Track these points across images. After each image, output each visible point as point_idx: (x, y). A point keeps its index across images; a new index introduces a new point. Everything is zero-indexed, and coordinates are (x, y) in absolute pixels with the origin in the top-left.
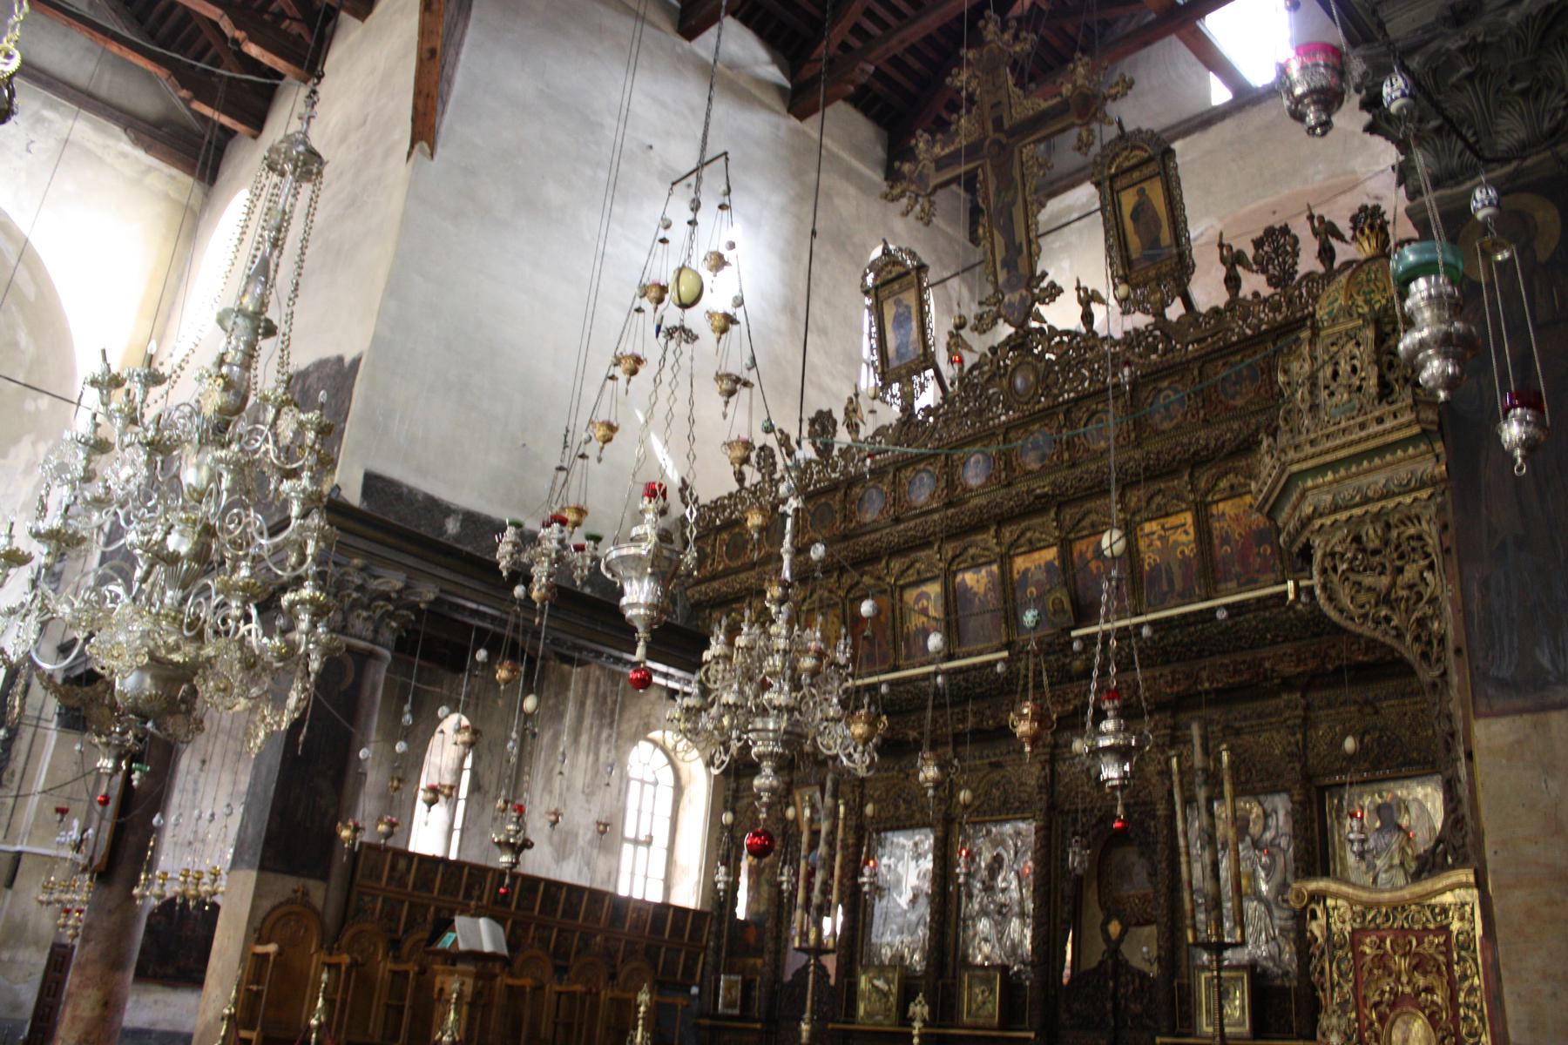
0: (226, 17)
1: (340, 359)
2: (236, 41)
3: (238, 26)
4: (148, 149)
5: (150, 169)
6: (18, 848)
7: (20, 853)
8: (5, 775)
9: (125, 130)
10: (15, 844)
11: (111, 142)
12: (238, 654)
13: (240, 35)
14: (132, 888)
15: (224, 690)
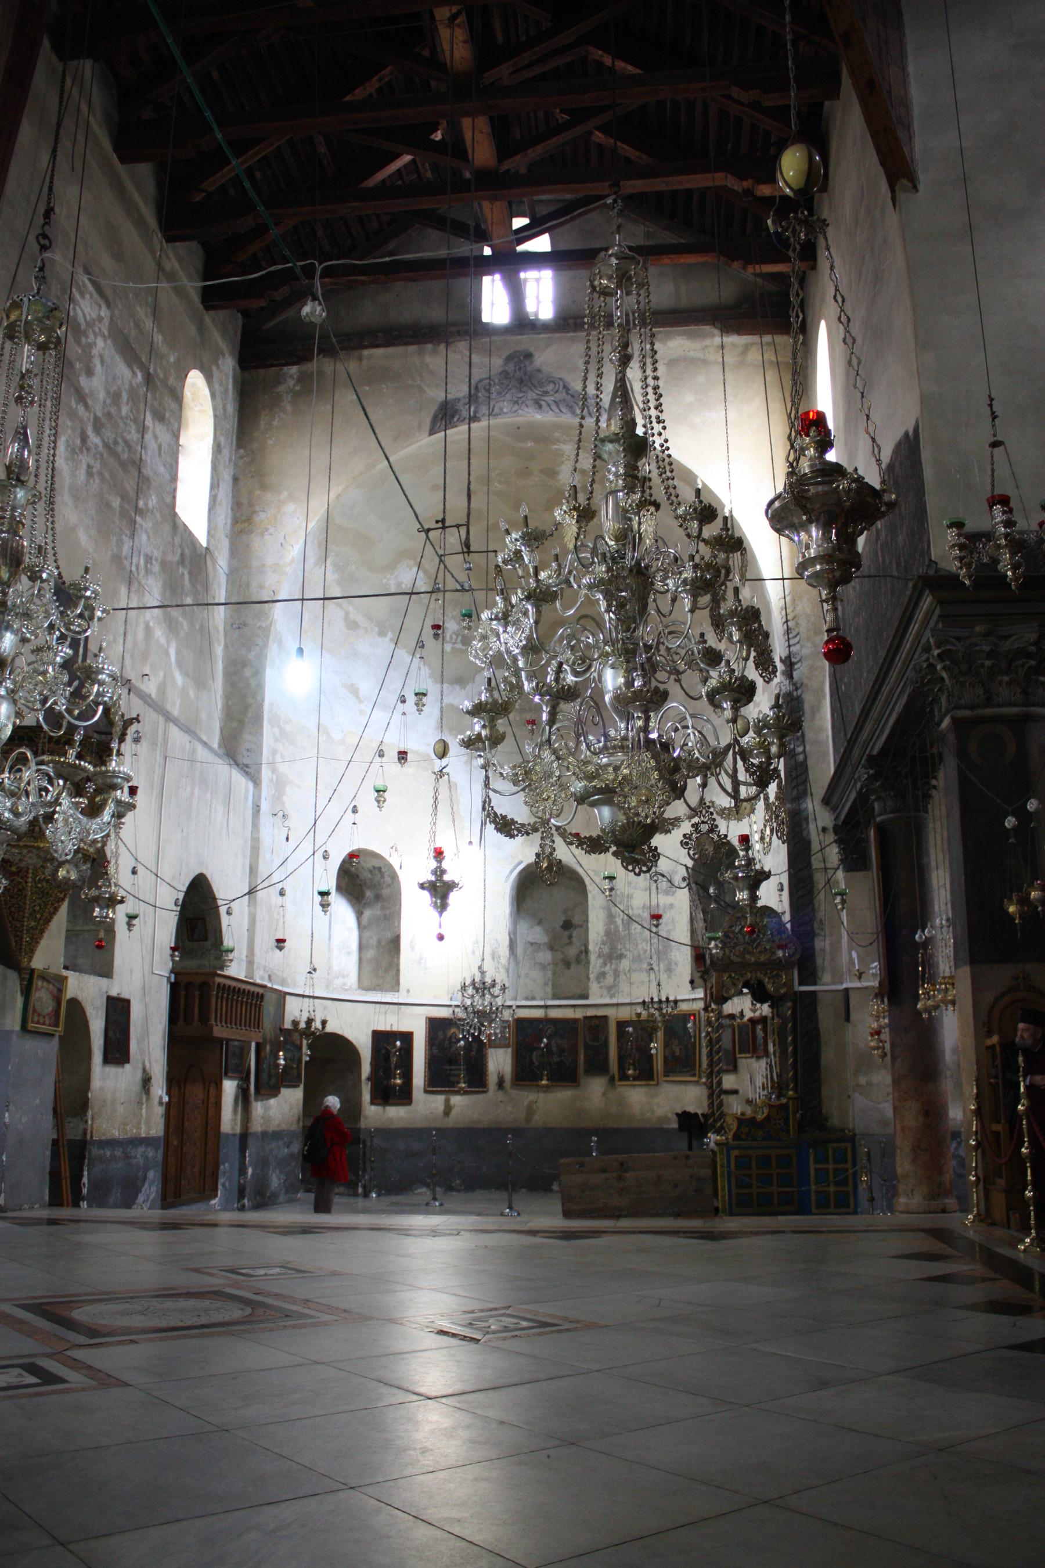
0: (729, 176)
1: (906, 434)
2: (748, 192)
3: (742, 178)
4: (739, 330)
5: (747, 348)
6: (844, 986)
7: (847, 990)
8: (816, 925)
9: (714, 325)
10: (842, 983)
11: (707, 342)
12: (653, 763)
13: (747, 184)
14: (916, 1004)
15: (647, 801)
